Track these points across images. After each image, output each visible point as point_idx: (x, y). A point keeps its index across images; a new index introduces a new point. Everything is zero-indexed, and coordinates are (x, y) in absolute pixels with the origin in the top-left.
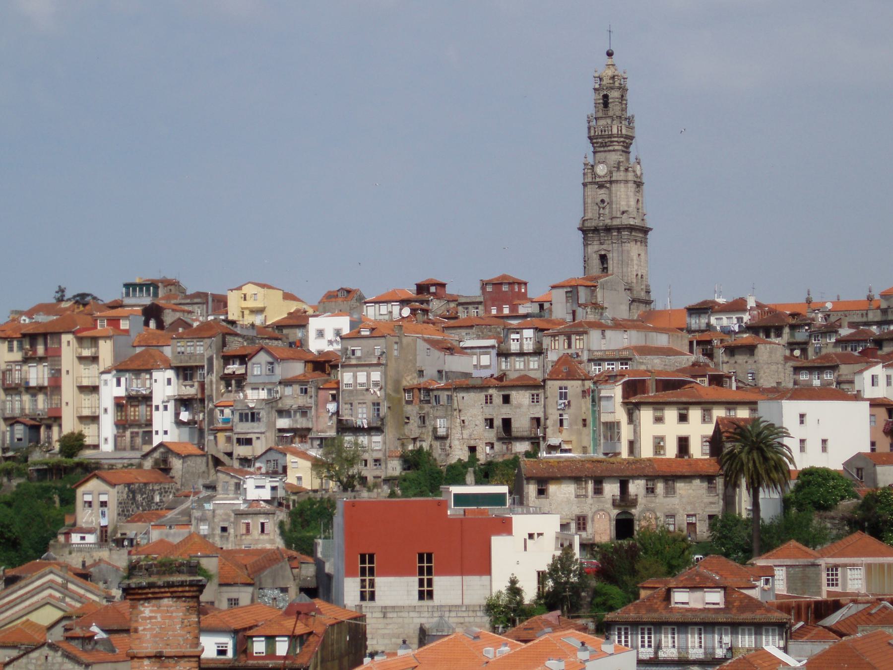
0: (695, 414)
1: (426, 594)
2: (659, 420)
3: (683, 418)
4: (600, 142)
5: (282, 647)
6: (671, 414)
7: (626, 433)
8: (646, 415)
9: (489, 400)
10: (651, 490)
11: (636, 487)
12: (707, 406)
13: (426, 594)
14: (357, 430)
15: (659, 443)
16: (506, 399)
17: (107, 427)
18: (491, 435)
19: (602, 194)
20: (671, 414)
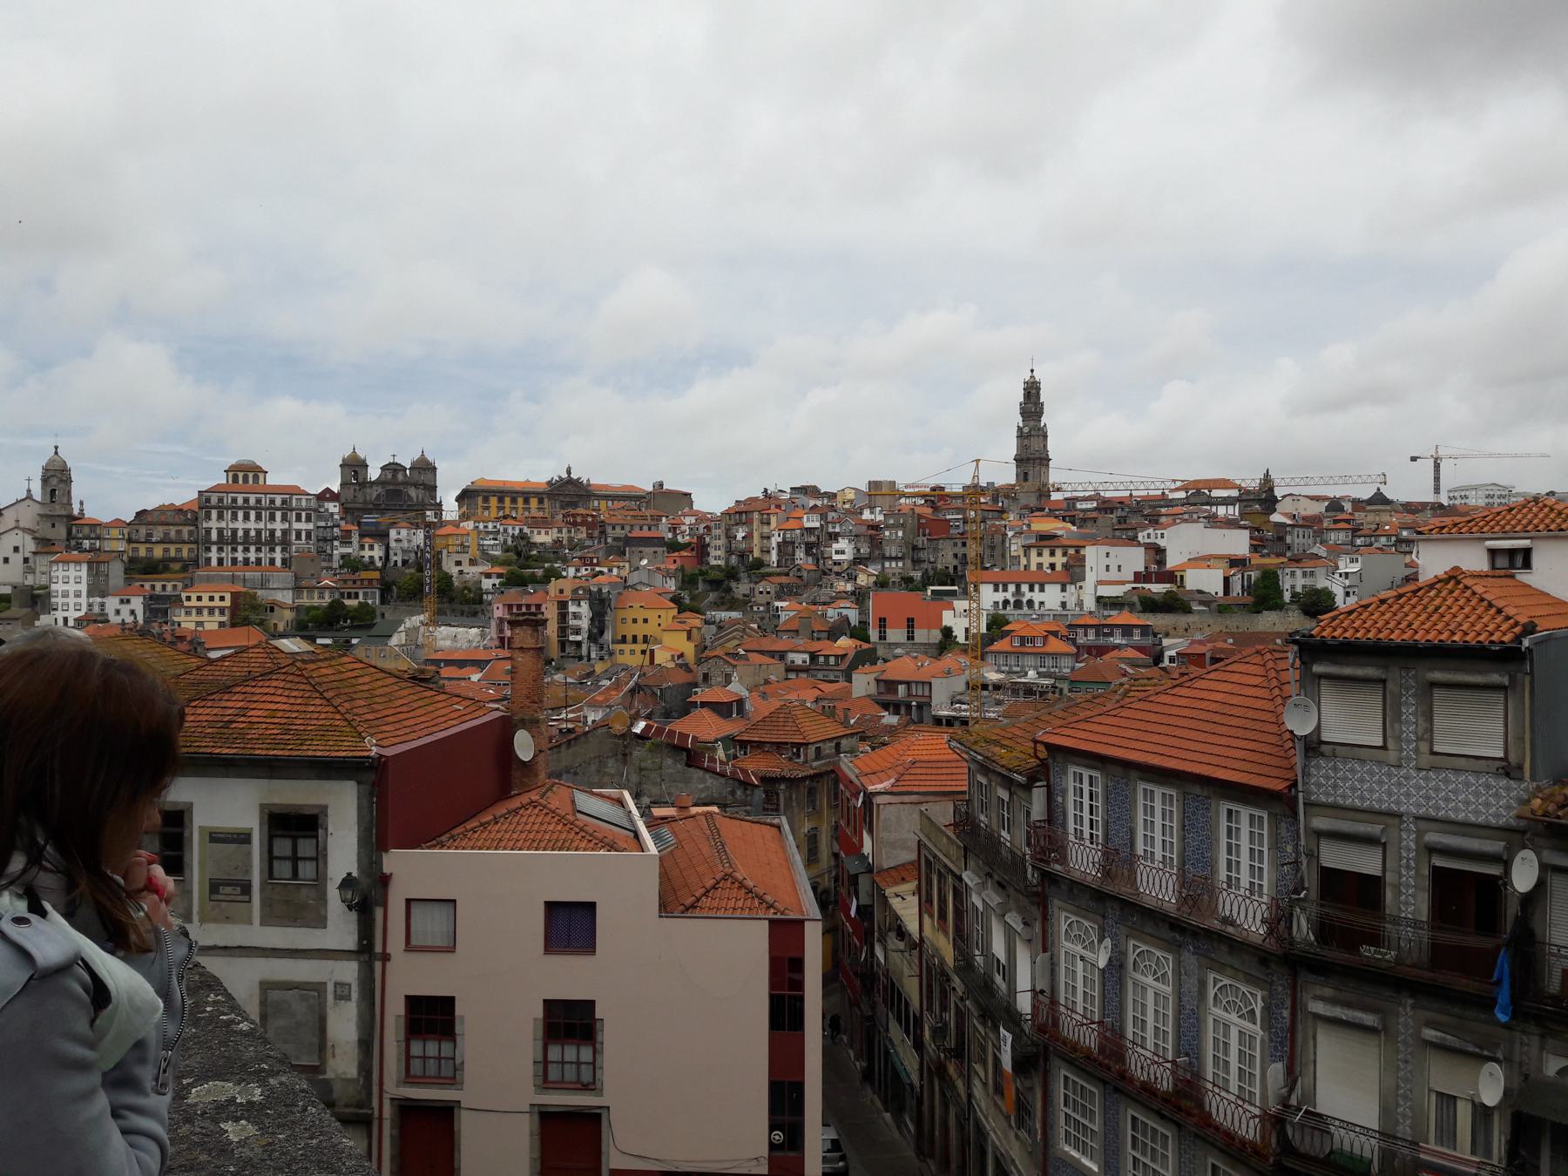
0: (1059, 552)
1: (910, 637)
2: (1040, 555)
3: (1052, 554)
4: (1025, 413)
5: (832, 661)
6: (1046, 552)
7: (1024, 561)
8: (1034, 552)
9: (955, 545)
10: (1031, 589)
11: (1025, 588)
12: (1065, 548)
13: (910, 637)
14: (891, 559)
15: (1040, 565)
16: (964, 544)
17: (774, 556)
18: (955, 562)
19: (1026, 442)
20: (1046, 552)
